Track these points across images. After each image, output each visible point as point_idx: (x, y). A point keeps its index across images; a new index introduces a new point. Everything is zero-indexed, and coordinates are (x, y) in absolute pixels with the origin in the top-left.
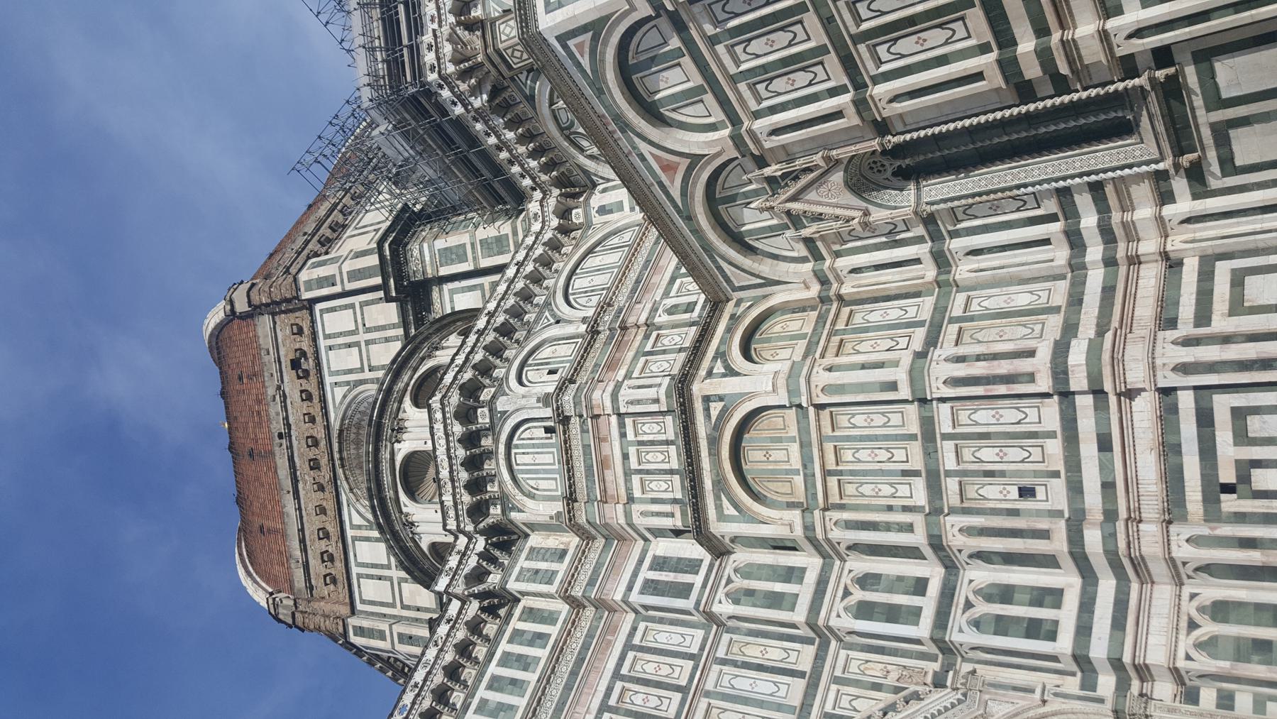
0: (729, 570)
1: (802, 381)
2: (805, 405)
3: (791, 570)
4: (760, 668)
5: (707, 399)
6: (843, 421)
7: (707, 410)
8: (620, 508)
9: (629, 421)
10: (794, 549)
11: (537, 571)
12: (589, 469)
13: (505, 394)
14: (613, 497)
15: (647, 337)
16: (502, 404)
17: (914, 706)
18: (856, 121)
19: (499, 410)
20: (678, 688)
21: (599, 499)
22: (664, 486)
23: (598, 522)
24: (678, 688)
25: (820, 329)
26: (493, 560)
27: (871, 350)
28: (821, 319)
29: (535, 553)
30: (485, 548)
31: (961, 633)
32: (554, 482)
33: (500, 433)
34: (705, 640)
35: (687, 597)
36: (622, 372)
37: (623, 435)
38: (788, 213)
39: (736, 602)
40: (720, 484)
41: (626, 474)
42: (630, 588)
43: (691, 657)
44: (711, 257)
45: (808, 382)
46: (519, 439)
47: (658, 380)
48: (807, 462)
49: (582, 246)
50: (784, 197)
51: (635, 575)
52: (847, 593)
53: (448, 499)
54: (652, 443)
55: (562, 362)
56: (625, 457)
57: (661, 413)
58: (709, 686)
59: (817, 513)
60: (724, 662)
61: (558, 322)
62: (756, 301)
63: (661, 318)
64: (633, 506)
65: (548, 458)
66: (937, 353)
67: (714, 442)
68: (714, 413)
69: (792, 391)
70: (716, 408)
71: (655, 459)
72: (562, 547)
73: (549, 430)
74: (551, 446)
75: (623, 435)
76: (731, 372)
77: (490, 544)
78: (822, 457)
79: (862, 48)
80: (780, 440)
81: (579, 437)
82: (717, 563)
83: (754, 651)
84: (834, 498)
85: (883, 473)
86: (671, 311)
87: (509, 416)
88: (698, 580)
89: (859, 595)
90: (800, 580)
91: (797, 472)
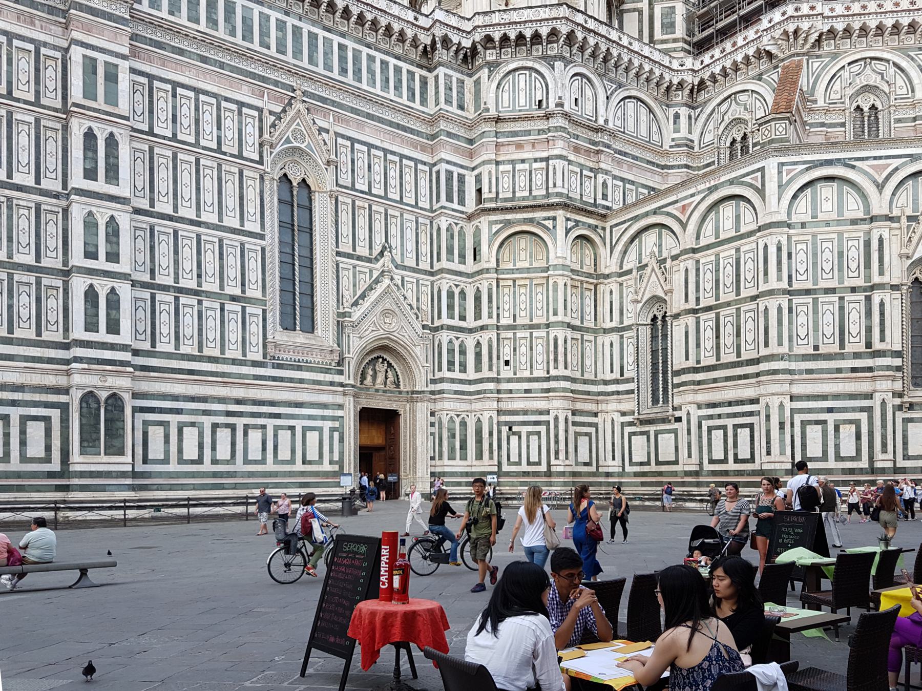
0: (461, 223)
1: (561, 272)
2: (549, 272)
3: (464, 257)
4: (417, 242)
5: (554, 219)
6: (539, 289)
7: (549, 219)
8: (493, 157)
9: (544, 164)
10: (475, 259)
11: (451, 89)
12: (515, 134)
13: (566, 66)
14: (499, 151)
15: (591, 170)
16: (559, 65)
17: (414, 317)
18: (682, 308)
19: (556, 63)
20: (401, 197)
21: (499, 140)
22: (506, 186)
23: (484, 140)
24: (401, 197)
25: (584, 275)
26: (457, 52)
27: (574, 301)
28: (590, 275)
29: (461, 82)
30: (464, 47)
31: (445, 337)
32: (507, 105)
33: (540, 63)
34: (425, 210)
35: (447, 200)
36: (572, 157)
37: (536, 160)
38: (646, 265)
39: (447, 230)
40: (508, 223)
41: (513, 161)
42: (448, 162)
43: (417, 203)
44: (631, 219)
45: (560, 275)
46: (536, 78)
47: (566, 186)
48: (520, 270)
49: (655, 103)
50: (655, 266)
51: (455, 164)
52: (457, 286)
53: (496, 18)
54: (531, 180)
55: (582, 108)
56: (523, 161)
57: (547, 188)
58: (406, 216)
59: (495, 275)
60: (417, 222)
61: (607, 98)
62: (603, 239)
63: (601, 178)
64: (494, 166)
65: (522, 102)
66: (569, 333)
67: (531, 221)
68: (546, 223)
69: (555, 267)
70: (549, 224)
71: (522, 181)
72: (466, 106)
73: (540, 101)
74: (531, 105)
75: (536, 160)
76: (568, 231)
77: (466, 52)
78: (522, 278)
79: (714, 315)
80: (531, 257)
81: (536, 128)
82: (464, 216)
83: (424, 238)
84: (501, 283)
85: (515, 306)
86: (605, 185)
87: (551, 72)
88: (455, 206)
89: (457, 291)
90: (460, 263)
91: (514, 265)
